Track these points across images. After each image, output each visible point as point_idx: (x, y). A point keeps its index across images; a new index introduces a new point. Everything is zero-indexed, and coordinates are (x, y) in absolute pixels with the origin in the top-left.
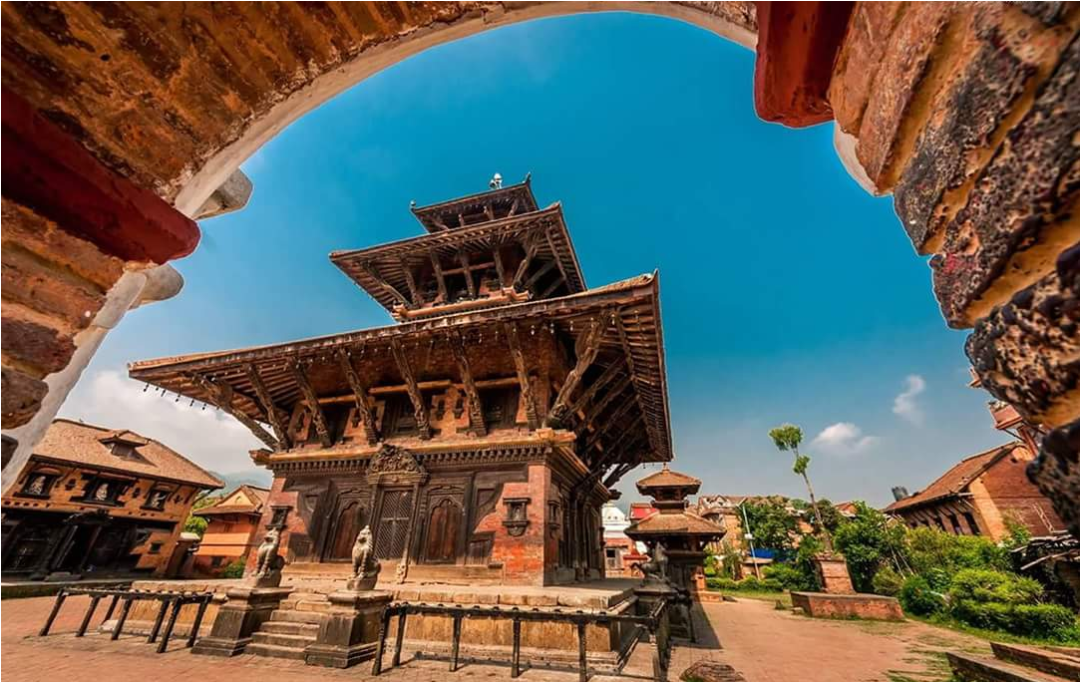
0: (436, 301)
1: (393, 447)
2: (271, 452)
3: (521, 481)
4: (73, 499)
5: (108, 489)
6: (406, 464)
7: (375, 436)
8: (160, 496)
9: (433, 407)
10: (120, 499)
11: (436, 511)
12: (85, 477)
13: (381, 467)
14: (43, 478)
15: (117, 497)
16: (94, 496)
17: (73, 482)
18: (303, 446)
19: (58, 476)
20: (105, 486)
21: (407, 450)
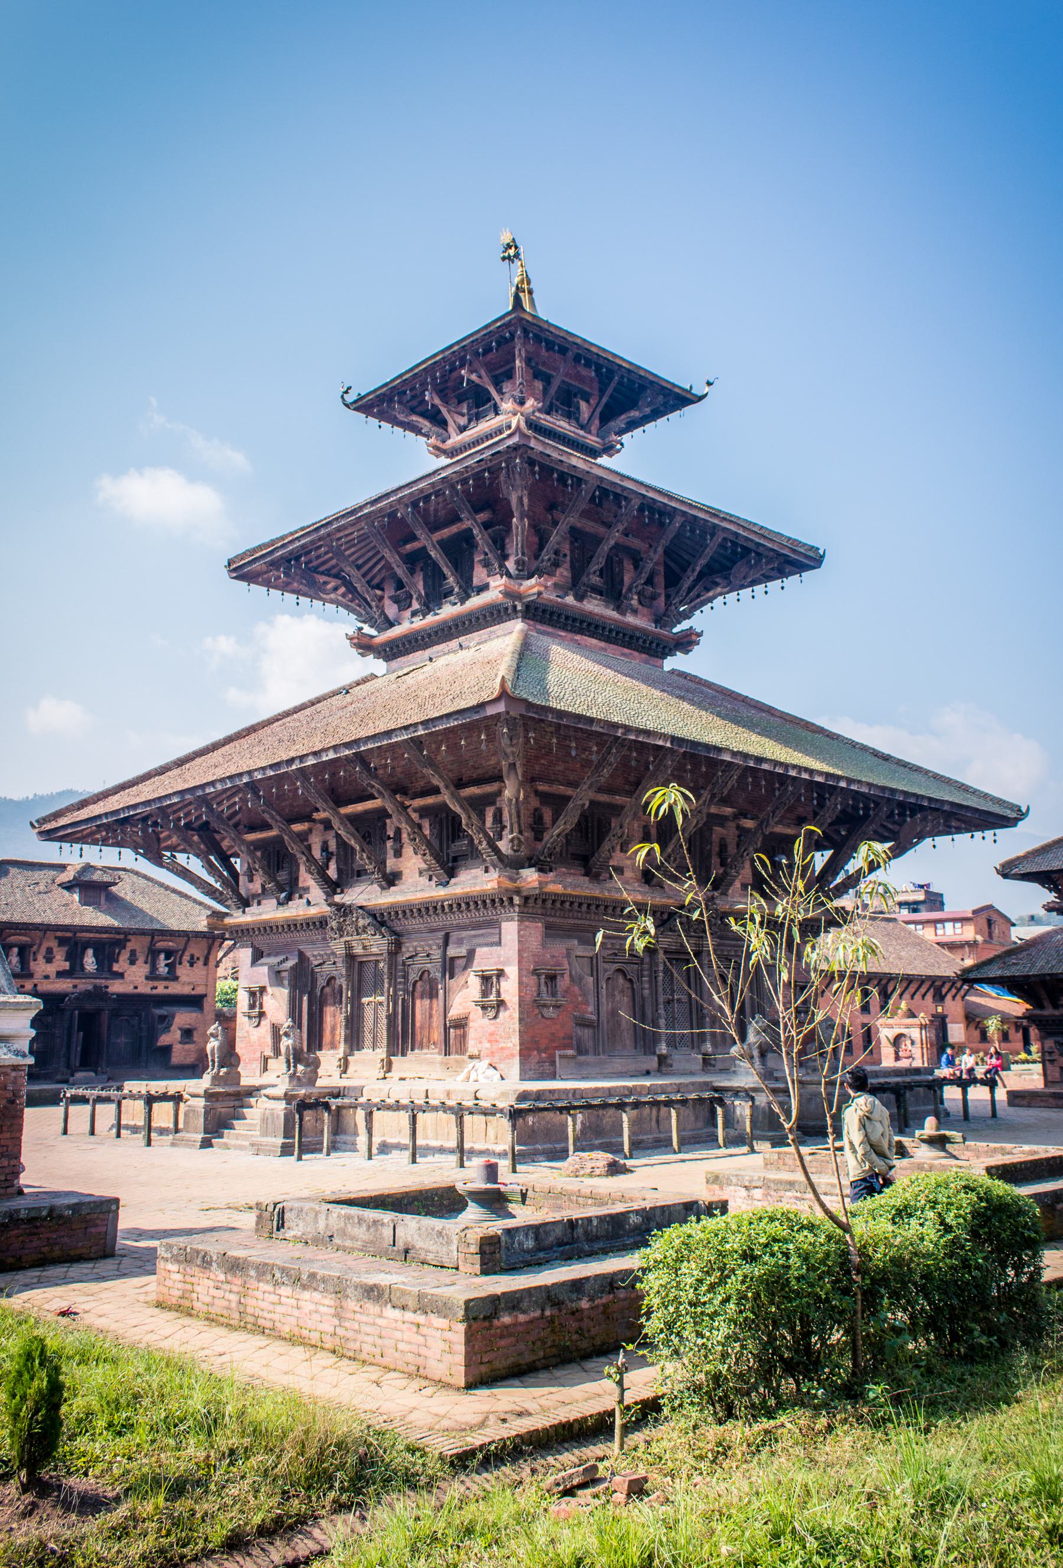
0: (416, 605)
1: (343, 905)
2: (227, 914)
3: (492, 944)
4: (60, 974)
5: (95, 955)
6: (365, 927)
7: (332, 887)
8: (167, 958)
9: (389, 838)
10: (116, 968)
11: (419, 984)
12: (62, 941)
13: (340, 929)
14: (16, 950)
15: (110, 967)
16: (83, 968)
17: (50, 951)
18: (259, 903)
19: (31, 946)
20: (90, 952)
21: (361, 907)
